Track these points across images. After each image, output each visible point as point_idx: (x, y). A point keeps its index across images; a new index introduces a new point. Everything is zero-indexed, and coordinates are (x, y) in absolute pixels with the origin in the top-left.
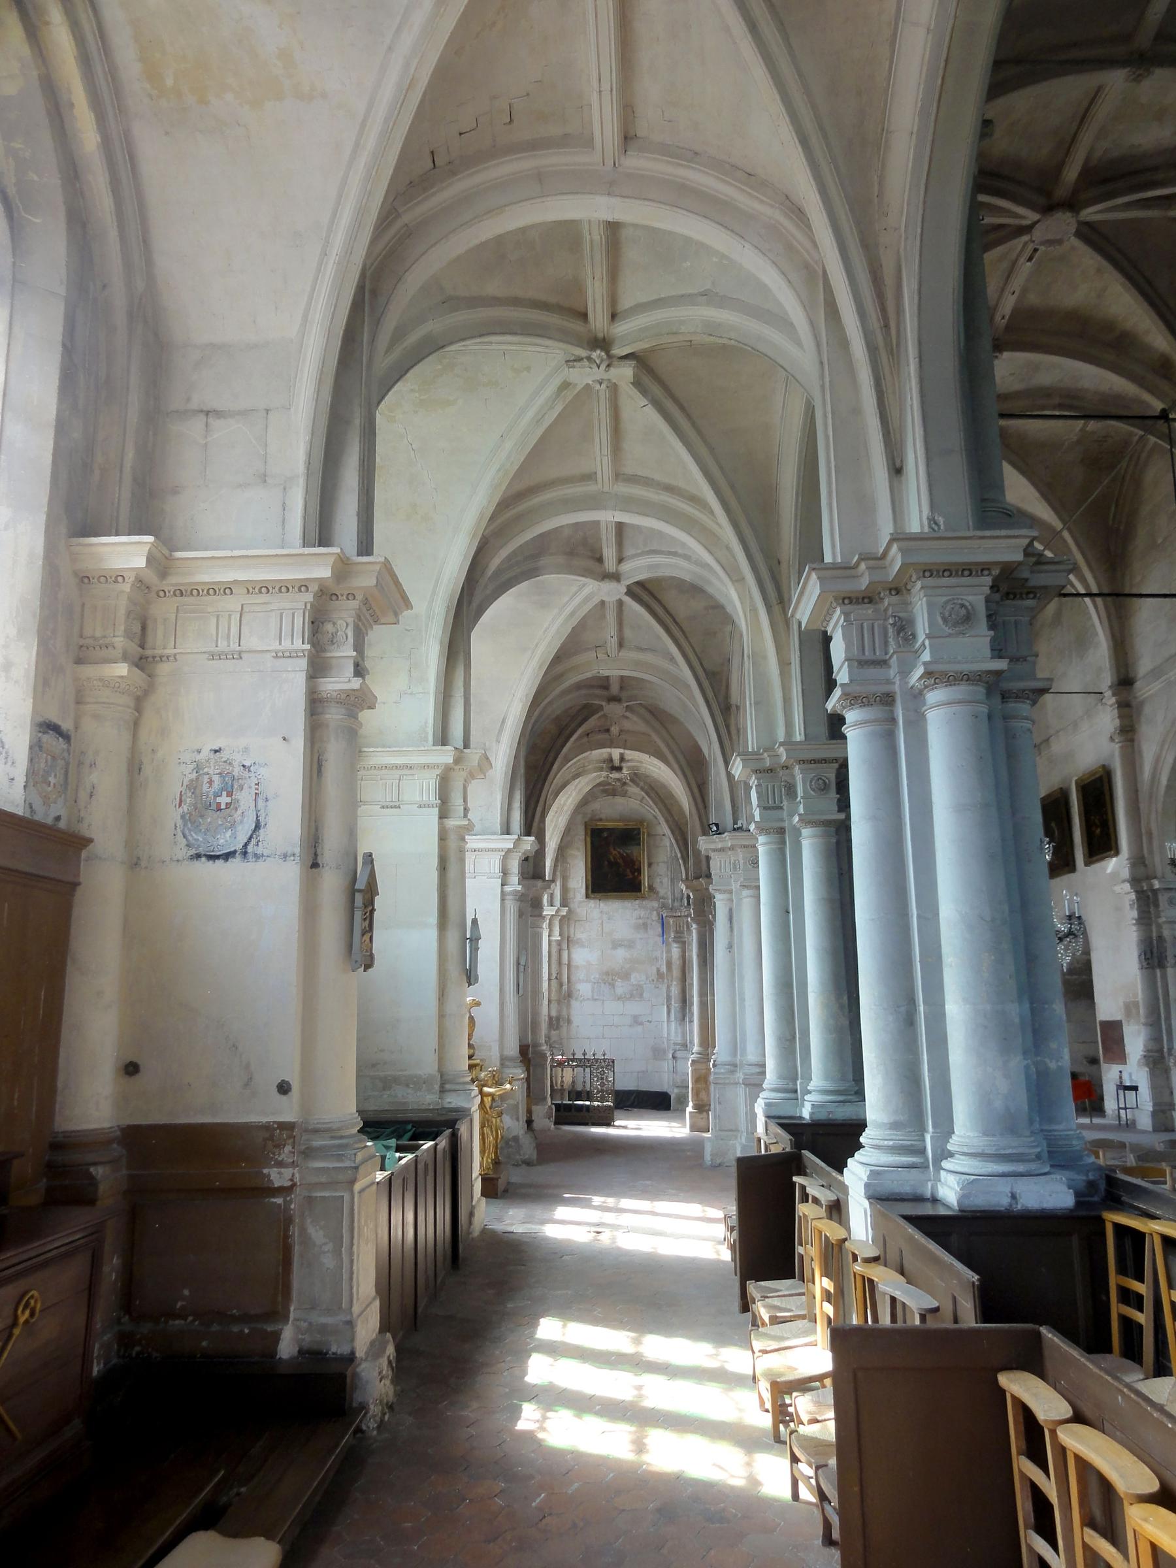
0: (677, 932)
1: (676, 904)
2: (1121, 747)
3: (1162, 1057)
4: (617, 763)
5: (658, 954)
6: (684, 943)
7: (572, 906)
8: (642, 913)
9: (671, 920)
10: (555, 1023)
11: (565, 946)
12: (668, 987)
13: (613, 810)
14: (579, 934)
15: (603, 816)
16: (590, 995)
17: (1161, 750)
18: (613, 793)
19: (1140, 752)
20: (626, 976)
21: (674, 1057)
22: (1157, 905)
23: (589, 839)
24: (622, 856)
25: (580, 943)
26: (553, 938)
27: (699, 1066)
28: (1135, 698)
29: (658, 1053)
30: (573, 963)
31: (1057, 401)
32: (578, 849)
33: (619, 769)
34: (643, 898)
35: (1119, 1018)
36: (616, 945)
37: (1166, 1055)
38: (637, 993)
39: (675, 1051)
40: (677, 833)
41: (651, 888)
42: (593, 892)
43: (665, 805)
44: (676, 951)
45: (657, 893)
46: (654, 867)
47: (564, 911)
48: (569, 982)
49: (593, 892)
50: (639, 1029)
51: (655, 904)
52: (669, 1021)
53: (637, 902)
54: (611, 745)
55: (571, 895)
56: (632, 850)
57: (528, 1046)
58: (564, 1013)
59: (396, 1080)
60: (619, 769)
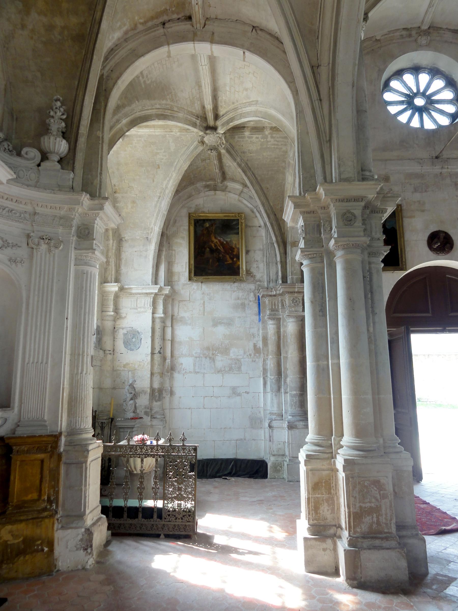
0: (272, 310)
1: (271, 285)
4: (211, 122)
5: (254, 330)
6: (279, 320)
7: (176, 288)
8: (240, 294)
9: (267, 300)
10: (157, 394)
11: (169, 323)
12: (264, 361)
13: (213, 204)
14: (182, 312)
15: (206, 210)
16: (192, 369)
18: (215, 189)
20: (225, 351)
21: (270, 427)
23: (192, 228)
24: (222, 244)
25: (183, 321)
26: (157, 315)
27: (317, 465)
29: (255, 422)
30: (177, 339)
32: (183, 238)
33: (214, 129)
34: (241, 281)
36: (216, 323)
38: (235, 367)
39: (271, 420)
40: (272, 216)
41: (249, 273)
42: (196, 275)
43: (262, 189)
44: (271, 327)
45: (254, 277)
46: (251, 254)
47: (167, 290)
48: (172, 356)
49: (196, 275)
50: (238, 399)
51: (252, 286)
52: (265, 392)
53: (236, 284)
54: (193, 37)
55: (175, 278)
56: (232, 239)
57: (56, 437)
58: (167, 385)
60: (214, 129)
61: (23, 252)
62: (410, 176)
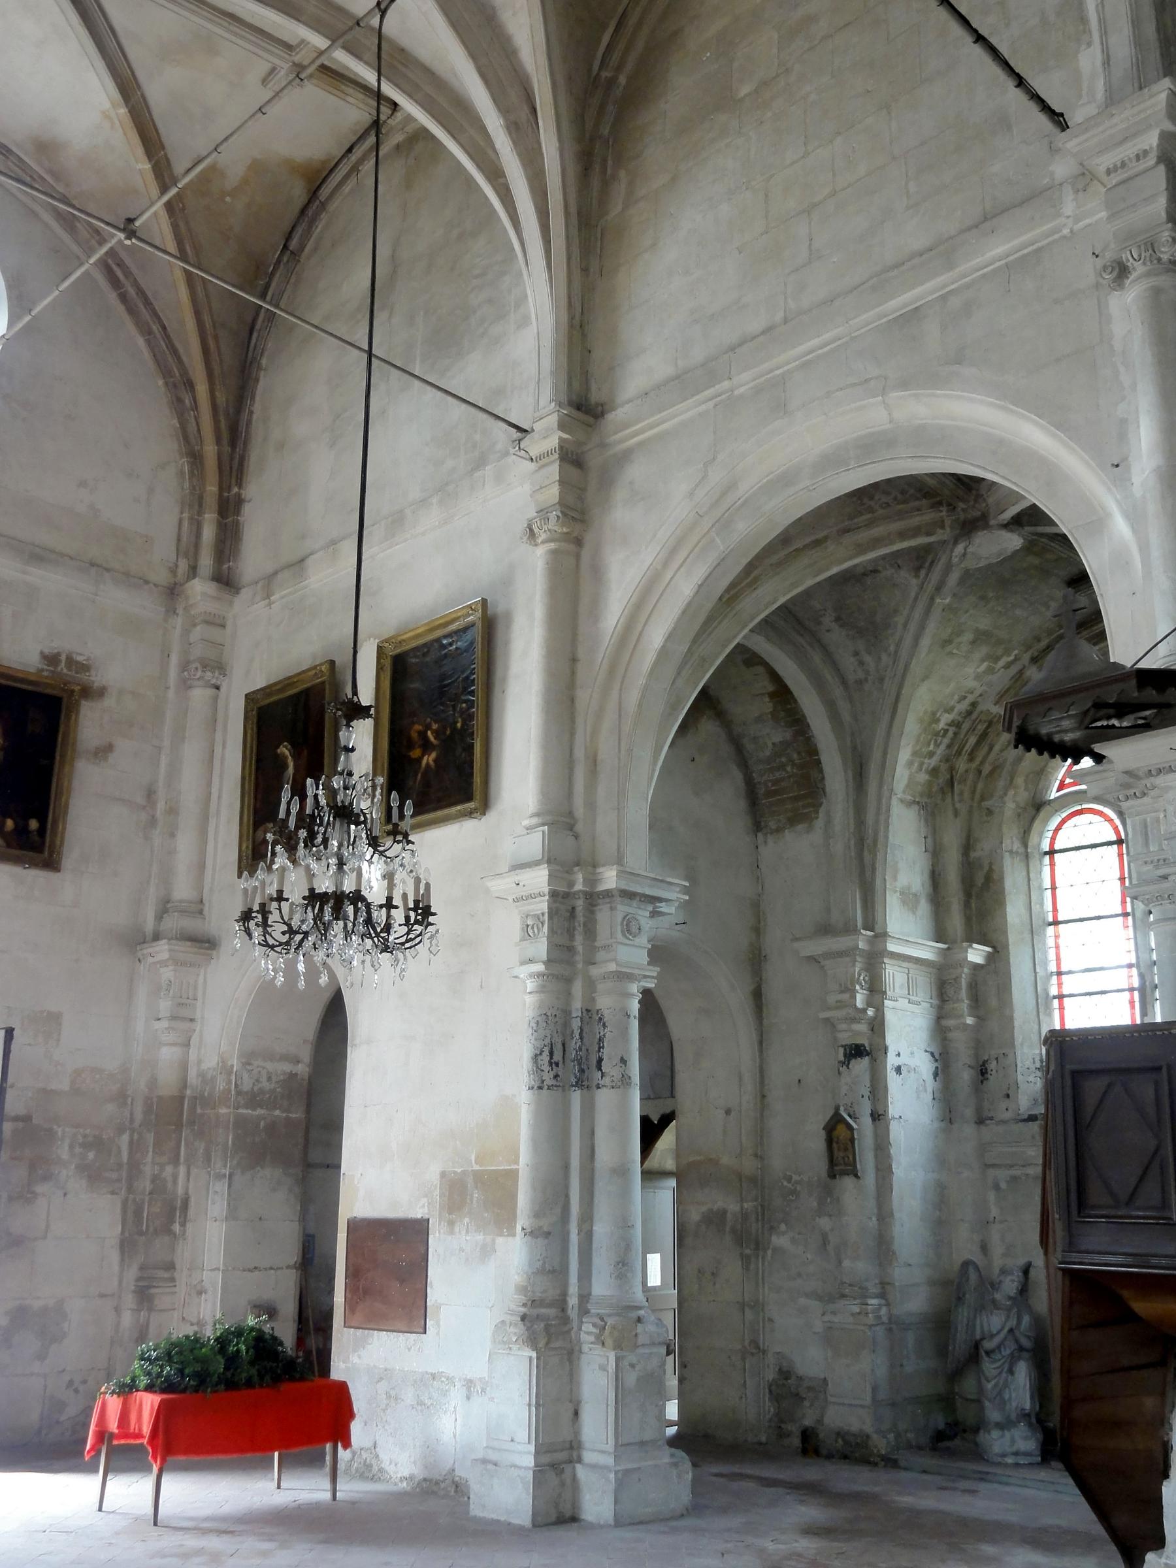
2: (554, 553)
3: (565, 1320)
17: (666, 564)
19: (598, 573)
22: (590, 932)
28: (603, 445)
35: (418, 1213)
37: (573, 1313)
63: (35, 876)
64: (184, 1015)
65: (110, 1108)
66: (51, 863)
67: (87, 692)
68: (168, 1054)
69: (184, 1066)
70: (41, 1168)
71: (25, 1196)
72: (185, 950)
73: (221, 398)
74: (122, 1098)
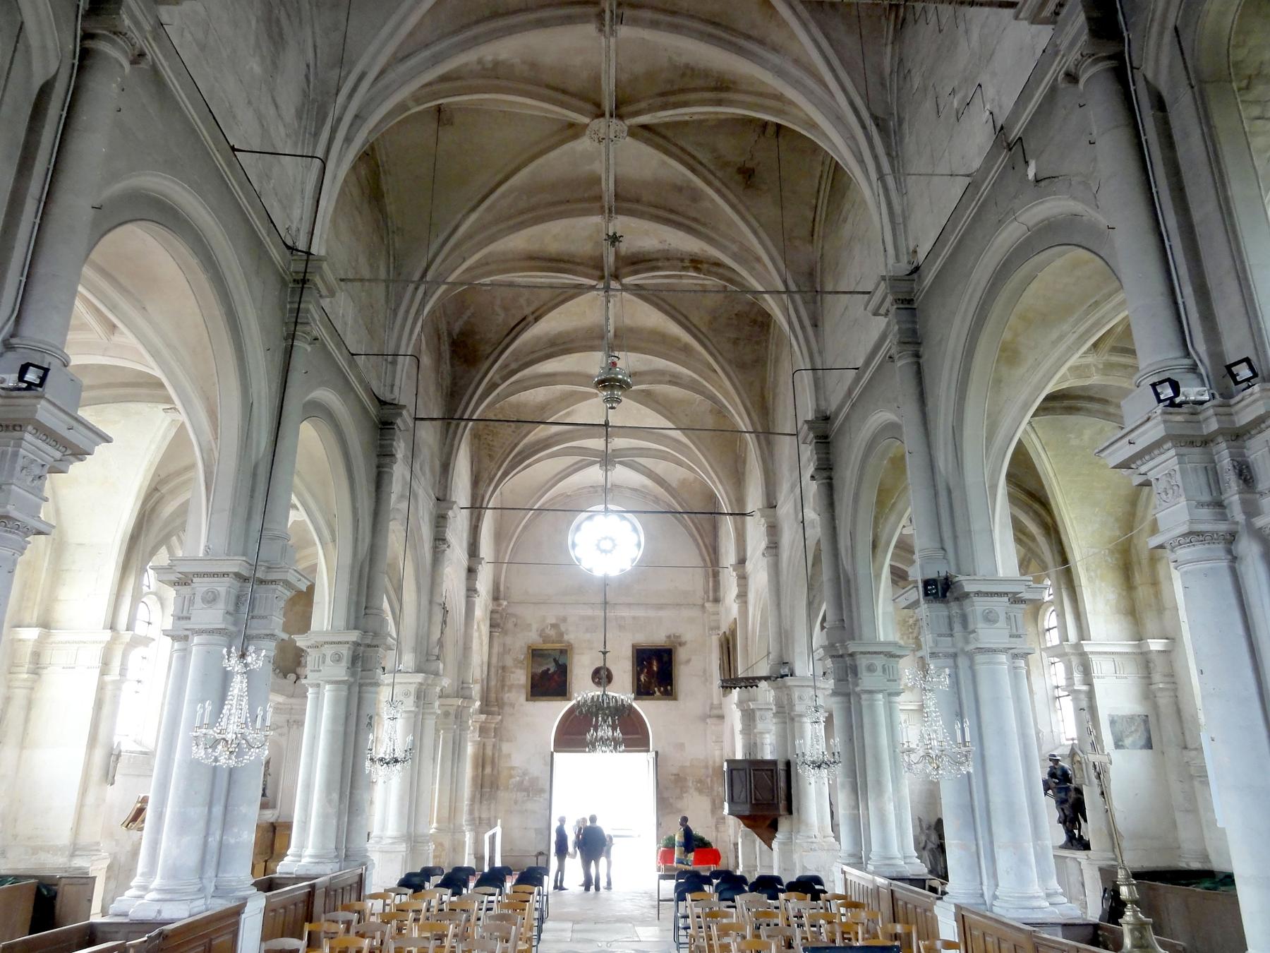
31: (668, 378)
59: (41, 848)
61: (285, 730)
62: (584, 618)
63: (672, 703)
64: (719, 741)
65: (703, 771)
66: (675, 699)
67: (681, 644)
68: (717, 753)
69: (722, 756)
70: (684, 789)
71: (680, 797)
72: (714, 720)
73: (707, 542)
74: (707, 767)
